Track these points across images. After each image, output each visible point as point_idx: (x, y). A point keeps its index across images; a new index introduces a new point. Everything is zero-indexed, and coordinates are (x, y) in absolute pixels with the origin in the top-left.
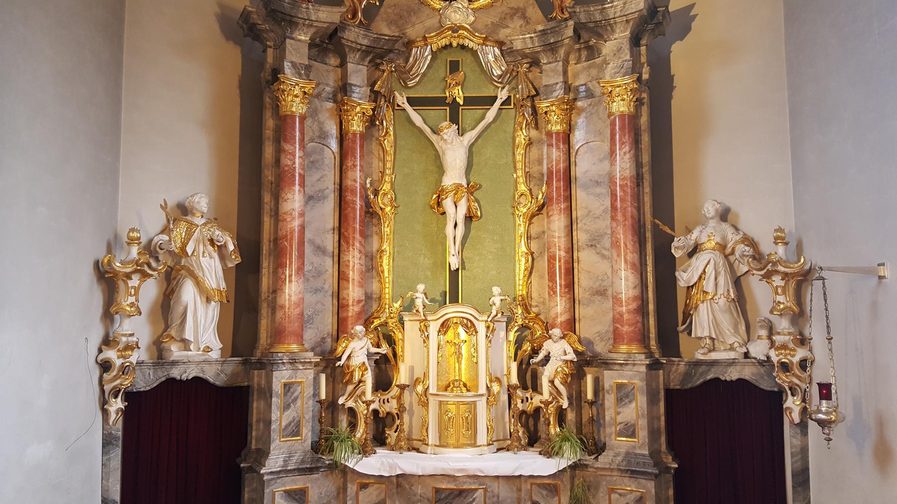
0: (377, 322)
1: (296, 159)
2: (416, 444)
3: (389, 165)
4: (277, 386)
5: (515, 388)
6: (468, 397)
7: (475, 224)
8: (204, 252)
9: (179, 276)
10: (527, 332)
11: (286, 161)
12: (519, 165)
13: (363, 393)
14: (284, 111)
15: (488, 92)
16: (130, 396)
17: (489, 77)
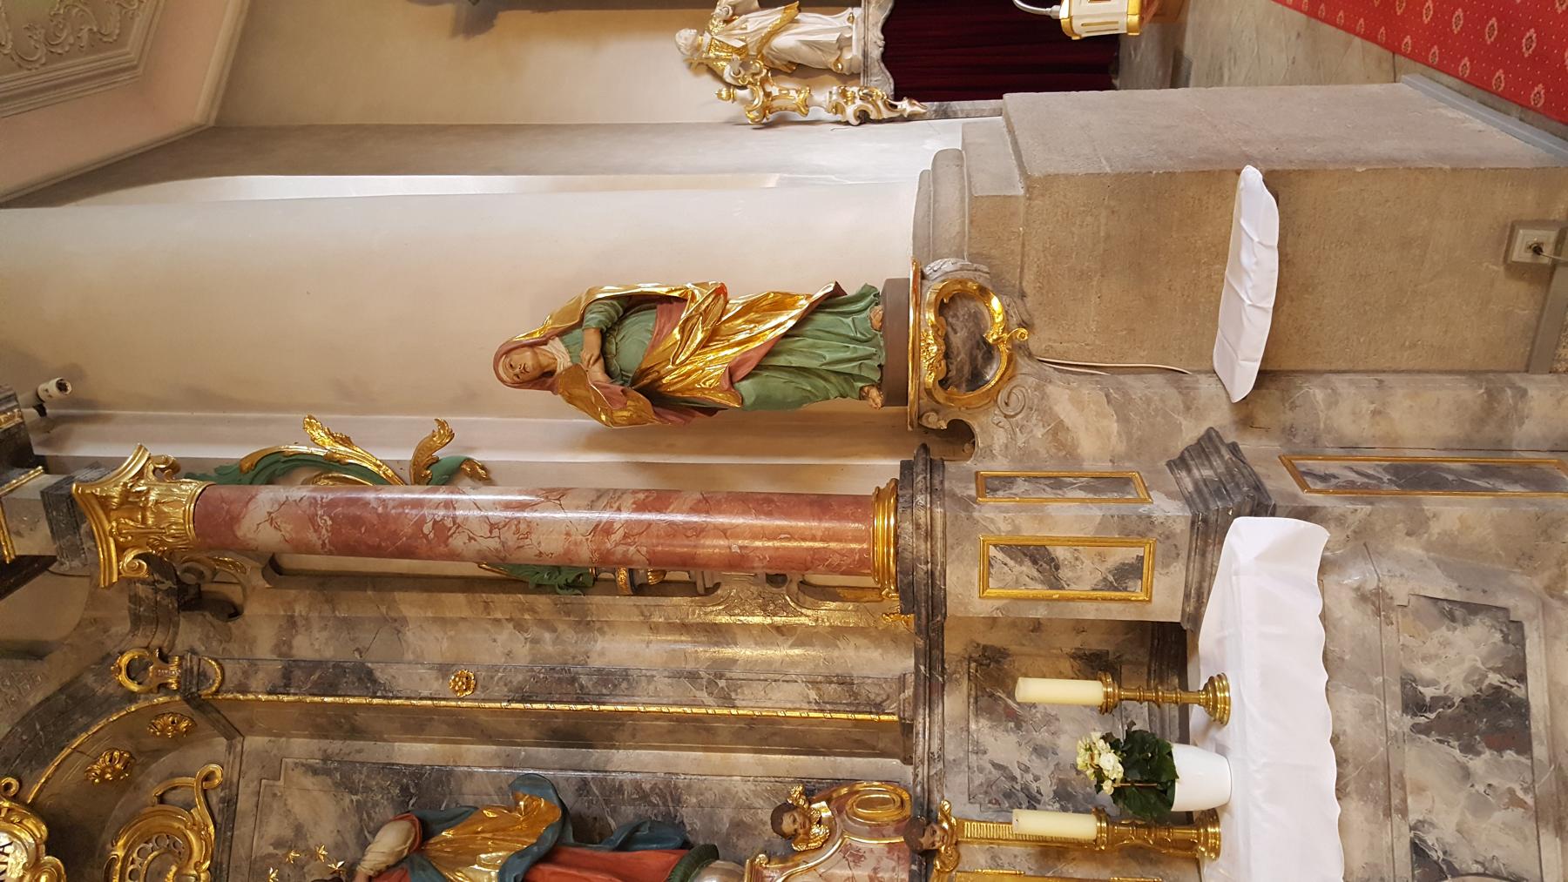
8: (742, 29)
9: (771, 57)
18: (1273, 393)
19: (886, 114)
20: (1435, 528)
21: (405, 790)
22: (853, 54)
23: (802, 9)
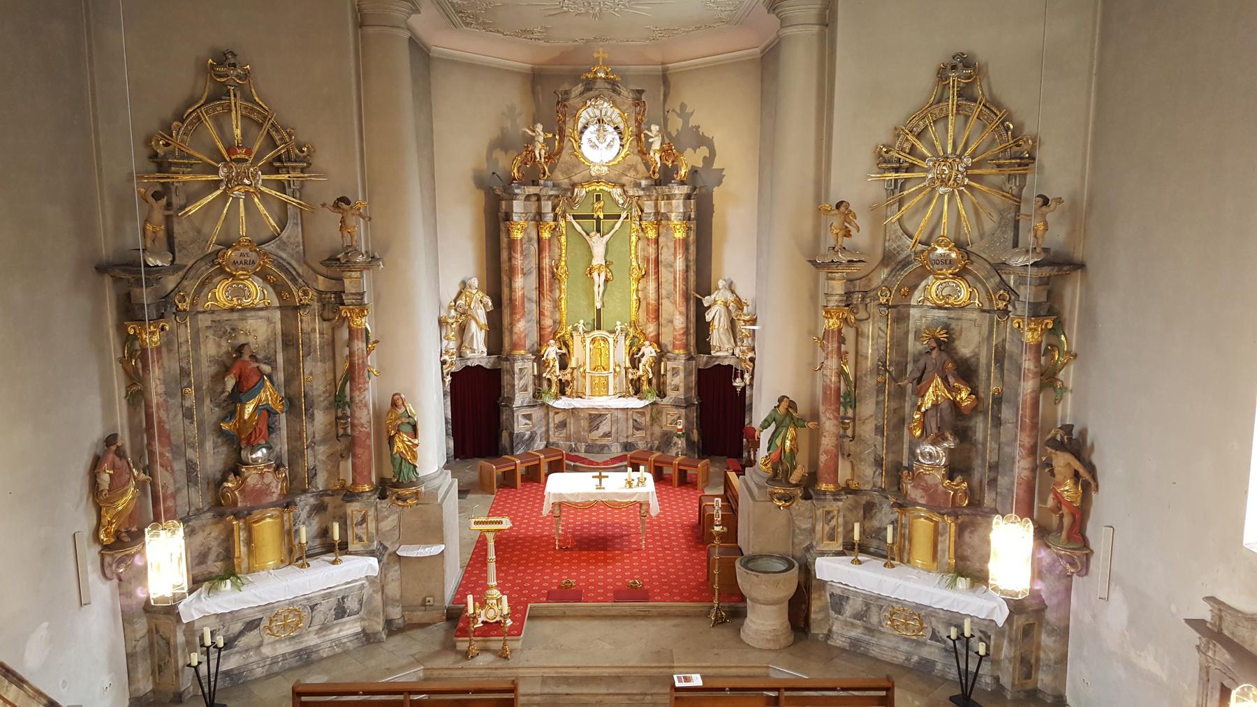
0: (559, 335)
1: (518, 261)
2: (580, 394)
3: (564, 251)
4: (517, 370)
5: (629, 368)
6: (605, 373)
7: (609, 283)
10: (636, 340)
11: (514, 262)
12: (633, 252)
13: (555, 372)
14: (512, 236)
15: (616, 211)
16: (453, 374)
17: (617, 203)
18: (397, 558)
19: (445, 372)
20: (375, 595)
21: (270, 358)
22: (469, 354)
23: (459, 611)
